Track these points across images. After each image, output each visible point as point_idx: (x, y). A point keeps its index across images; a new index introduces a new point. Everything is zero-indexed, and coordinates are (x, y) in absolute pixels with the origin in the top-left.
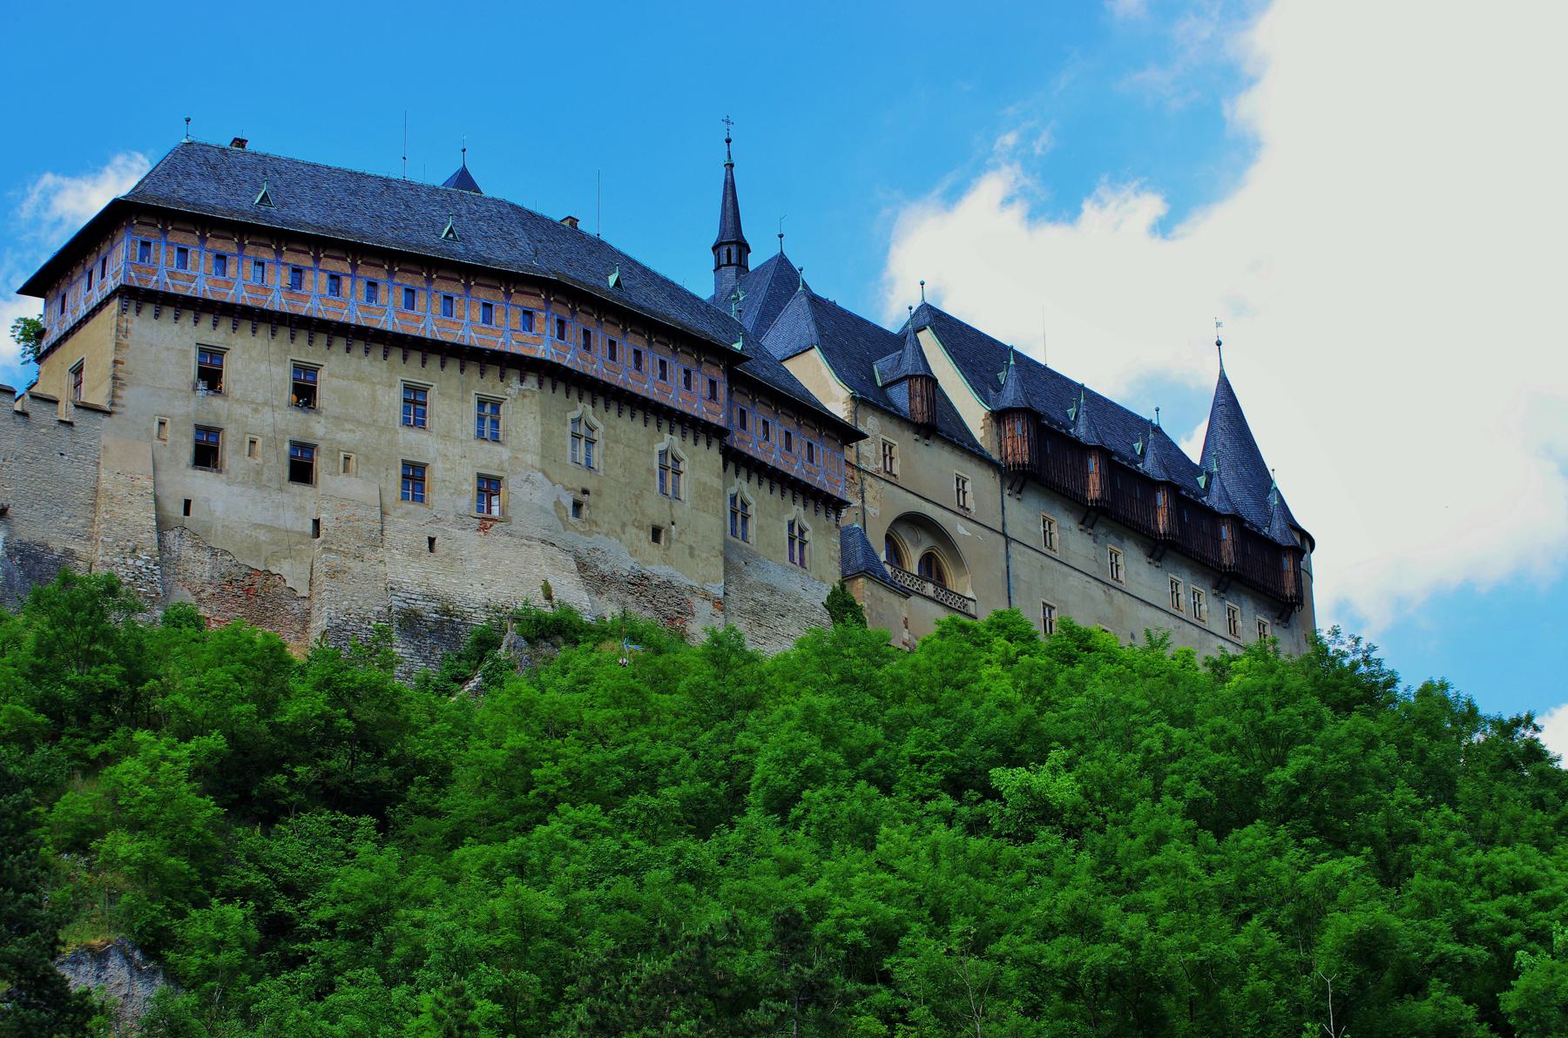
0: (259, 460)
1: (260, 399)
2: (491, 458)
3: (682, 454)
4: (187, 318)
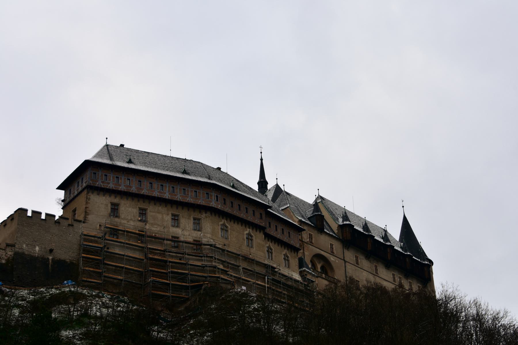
1: (129, 218)
3: (252, 234)
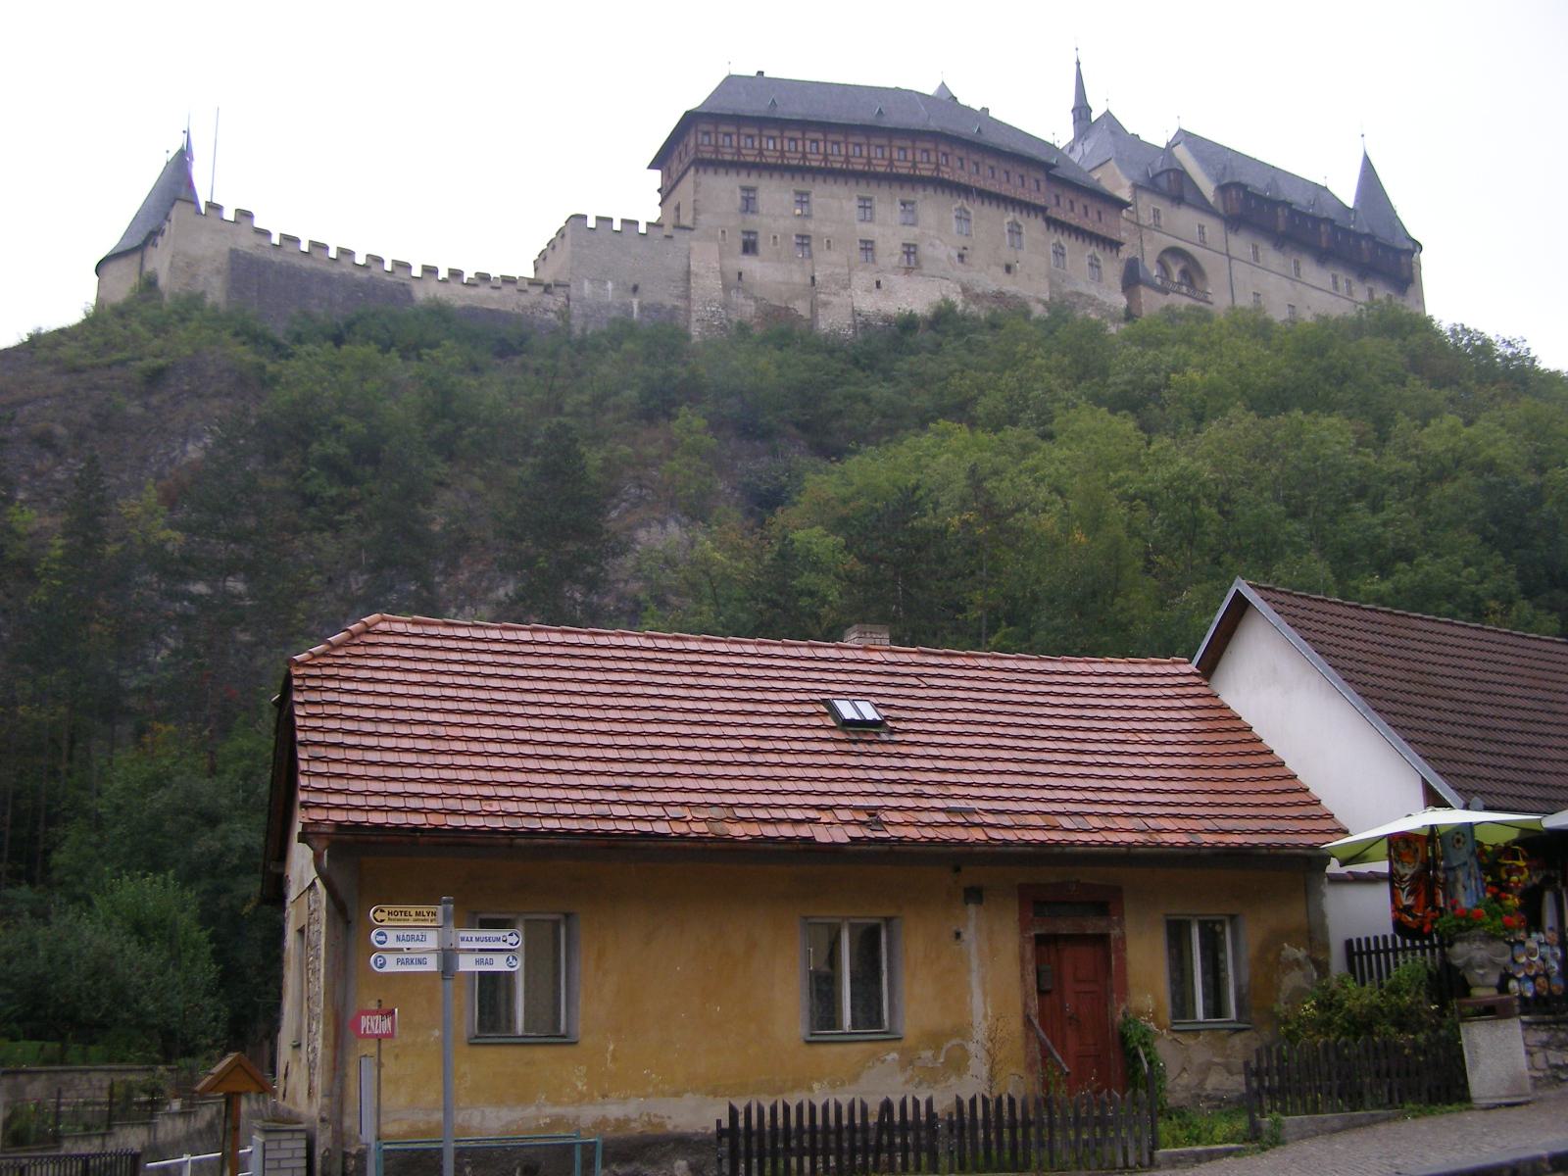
0: (779, 247)
2: (909, 234)
3: (1021, 223)
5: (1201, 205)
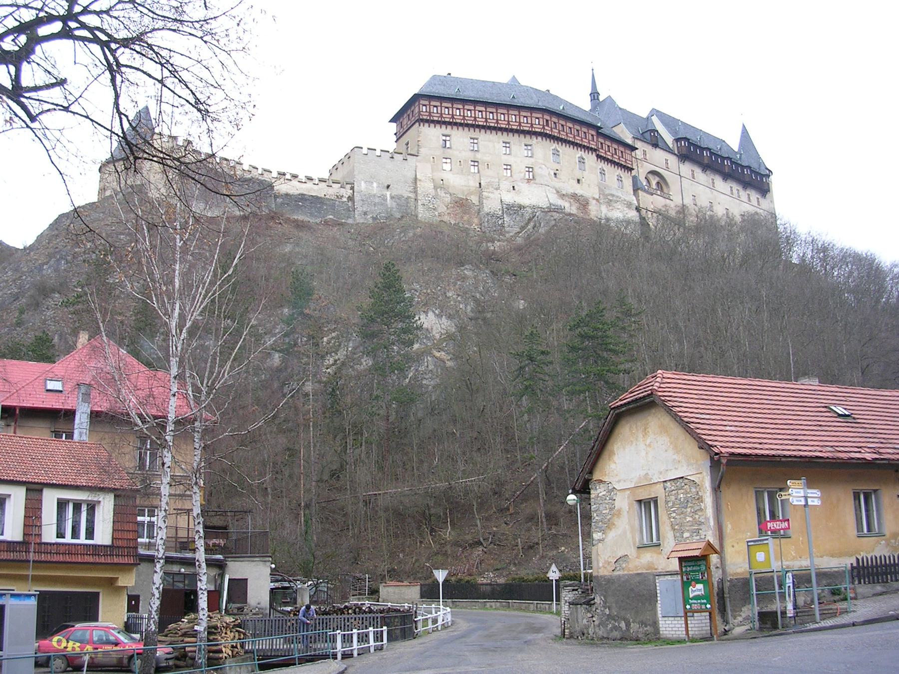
2: (529, 162)
4: (438, 126)
5: (671, 151)
